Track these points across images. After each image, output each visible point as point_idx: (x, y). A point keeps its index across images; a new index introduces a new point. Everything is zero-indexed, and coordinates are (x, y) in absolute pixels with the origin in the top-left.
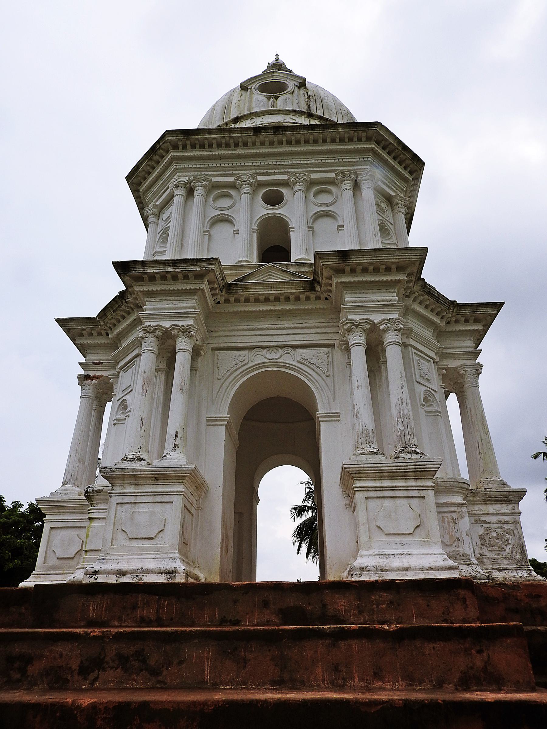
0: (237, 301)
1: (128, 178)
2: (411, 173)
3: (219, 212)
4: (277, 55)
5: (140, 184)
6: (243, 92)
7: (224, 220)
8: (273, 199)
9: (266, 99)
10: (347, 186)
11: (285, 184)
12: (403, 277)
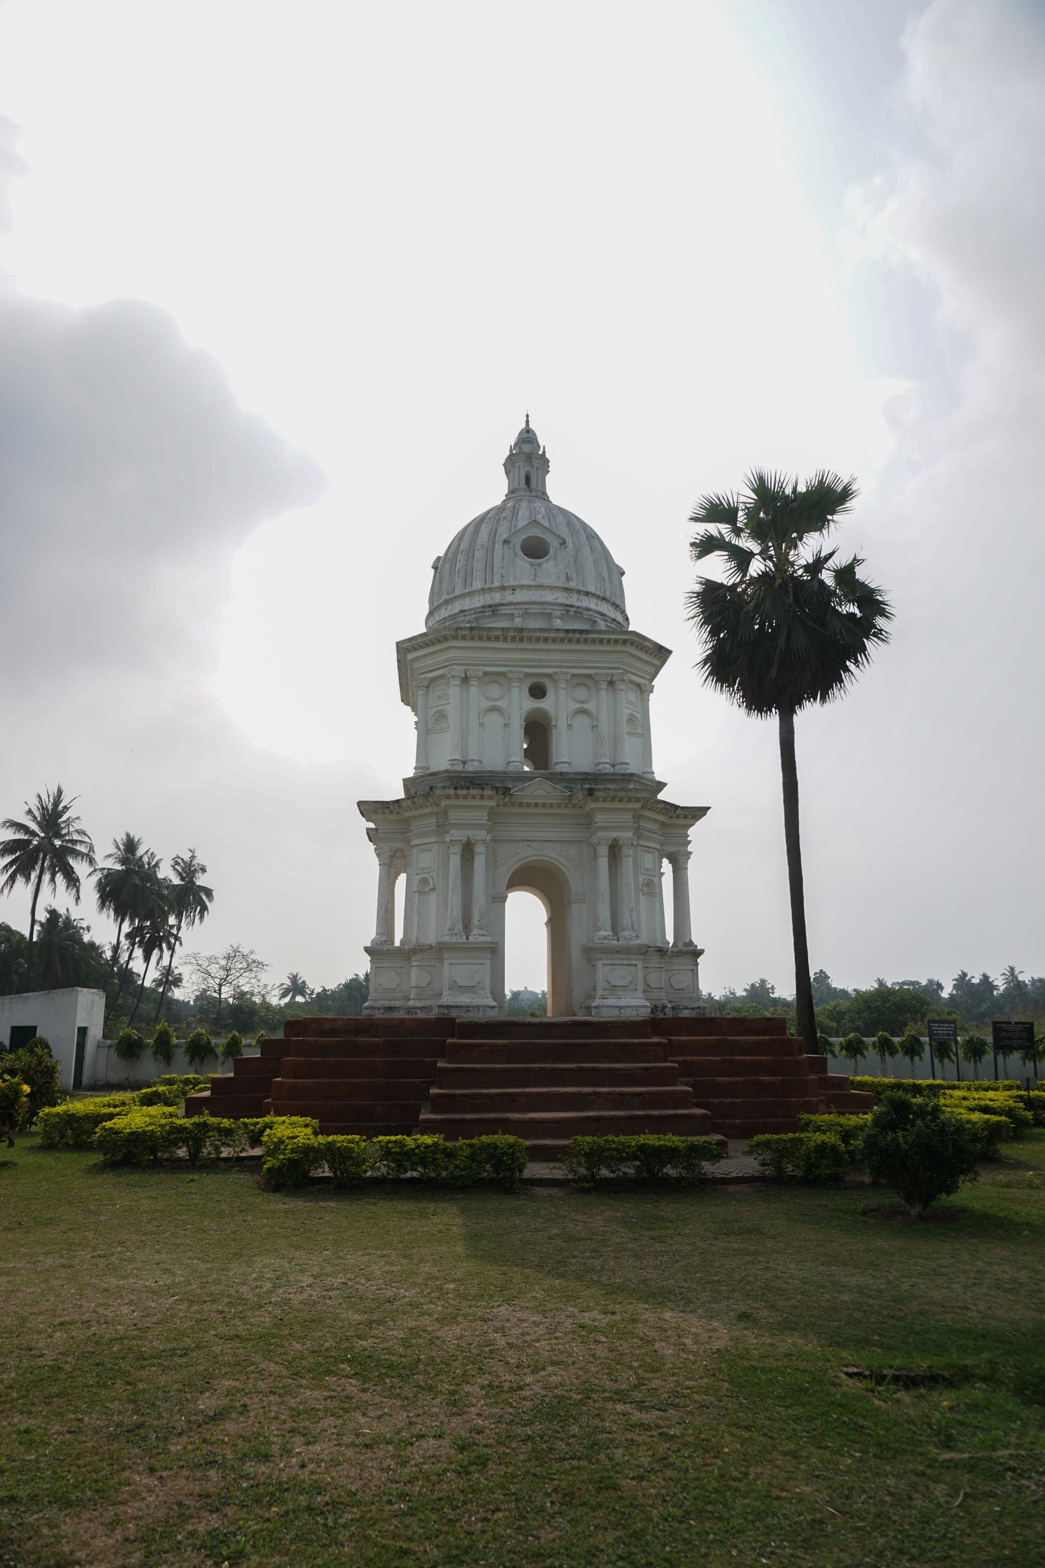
0: (513, 805)
1: (398, 644)
2: (660, 658)
3: (491, 703)
4: (527, 416)
5: (410, 651)
6: (506, 547)
7: (495, 709)
8: (538, 692)
9: (528, 566)
10: (604, 685)
11: (548, 675)
12: (638, 805)
